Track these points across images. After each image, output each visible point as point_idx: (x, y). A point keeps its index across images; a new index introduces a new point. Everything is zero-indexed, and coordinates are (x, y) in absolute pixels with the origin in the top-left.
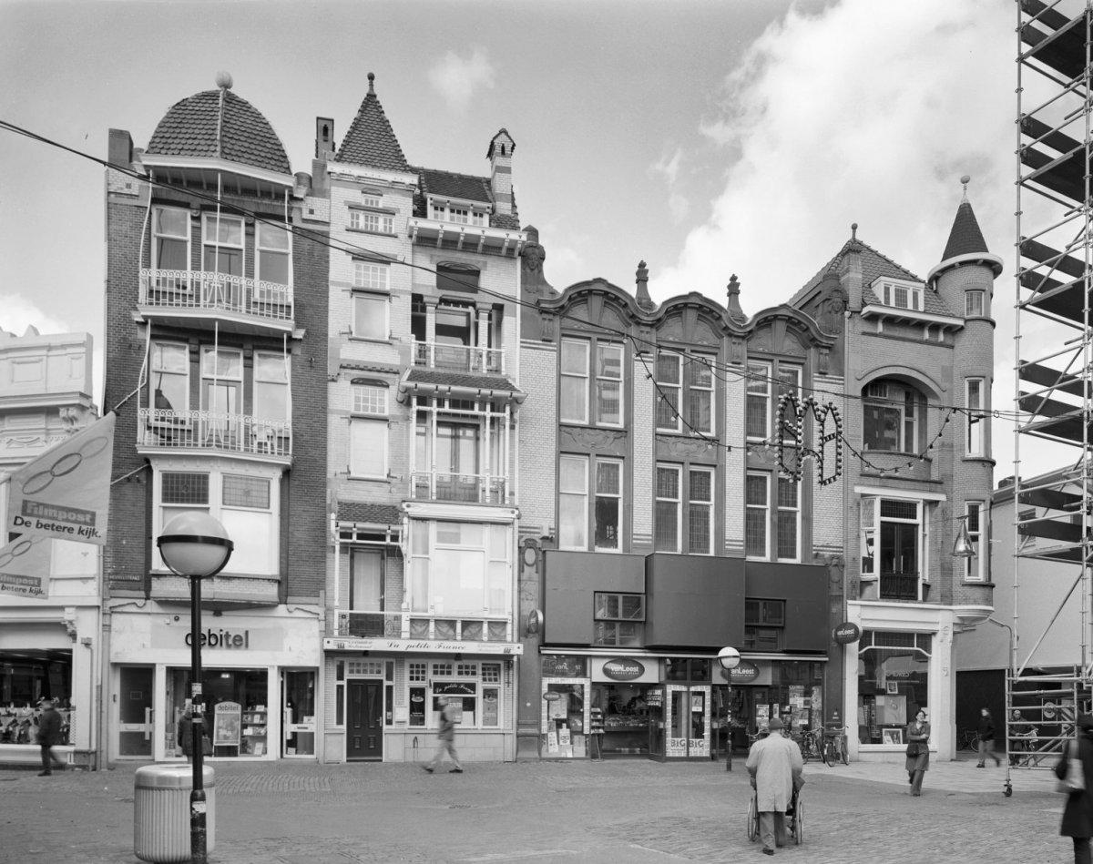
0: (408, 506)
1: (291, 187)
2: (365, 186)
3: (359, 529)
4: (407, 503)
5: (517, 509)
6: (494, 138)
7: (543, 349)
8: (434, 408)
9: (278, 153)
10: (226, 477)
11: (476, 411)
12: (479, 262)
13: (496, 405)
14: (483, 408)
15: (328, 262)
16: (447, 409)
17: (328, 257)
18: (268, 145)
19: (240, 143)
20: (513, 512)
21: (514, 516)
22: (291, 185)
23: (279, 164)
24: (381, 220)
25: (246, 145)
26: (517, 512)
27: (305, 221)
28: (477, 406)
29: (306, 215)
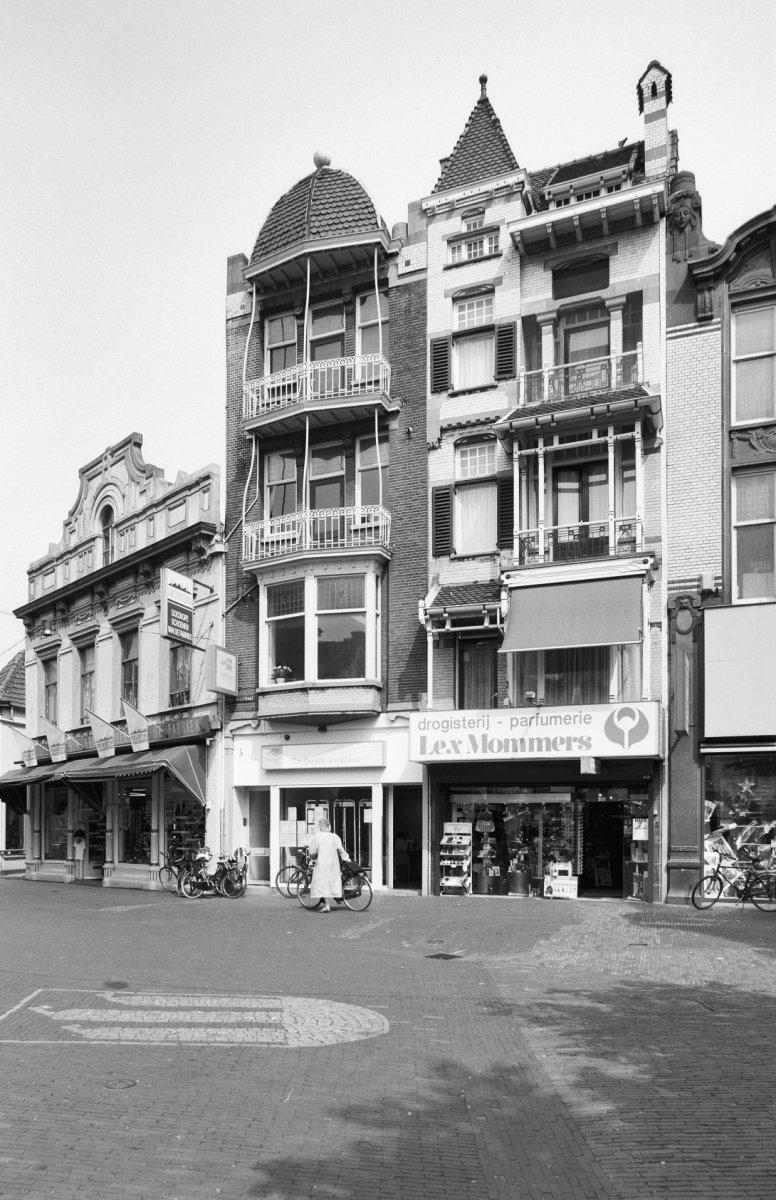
0: (508, 577)
1: (379, 243)
2: (465, 209)
3: (450, 614)
4: (506, 574)
5: (653, 556)
6: (641, 80)
7: (701, 333)
8: (541, 450)
9: (366, 211)
10: (321, 580)
11: (595, 439)
12: (606, 247)
13: (623, 422)
15: (425, 314)
16: (556, 445)
17: (425, 308)
18: (356, 207)
19: (327, 217)
20: (645, 562)
21: (647, 566)
22: (379, 240)
23: (367, 222)
24: (486, 243)
25: (334, 215)
26: (651, 561)
27: (401, 276)
28: (595, 434)
29: (403, 269)
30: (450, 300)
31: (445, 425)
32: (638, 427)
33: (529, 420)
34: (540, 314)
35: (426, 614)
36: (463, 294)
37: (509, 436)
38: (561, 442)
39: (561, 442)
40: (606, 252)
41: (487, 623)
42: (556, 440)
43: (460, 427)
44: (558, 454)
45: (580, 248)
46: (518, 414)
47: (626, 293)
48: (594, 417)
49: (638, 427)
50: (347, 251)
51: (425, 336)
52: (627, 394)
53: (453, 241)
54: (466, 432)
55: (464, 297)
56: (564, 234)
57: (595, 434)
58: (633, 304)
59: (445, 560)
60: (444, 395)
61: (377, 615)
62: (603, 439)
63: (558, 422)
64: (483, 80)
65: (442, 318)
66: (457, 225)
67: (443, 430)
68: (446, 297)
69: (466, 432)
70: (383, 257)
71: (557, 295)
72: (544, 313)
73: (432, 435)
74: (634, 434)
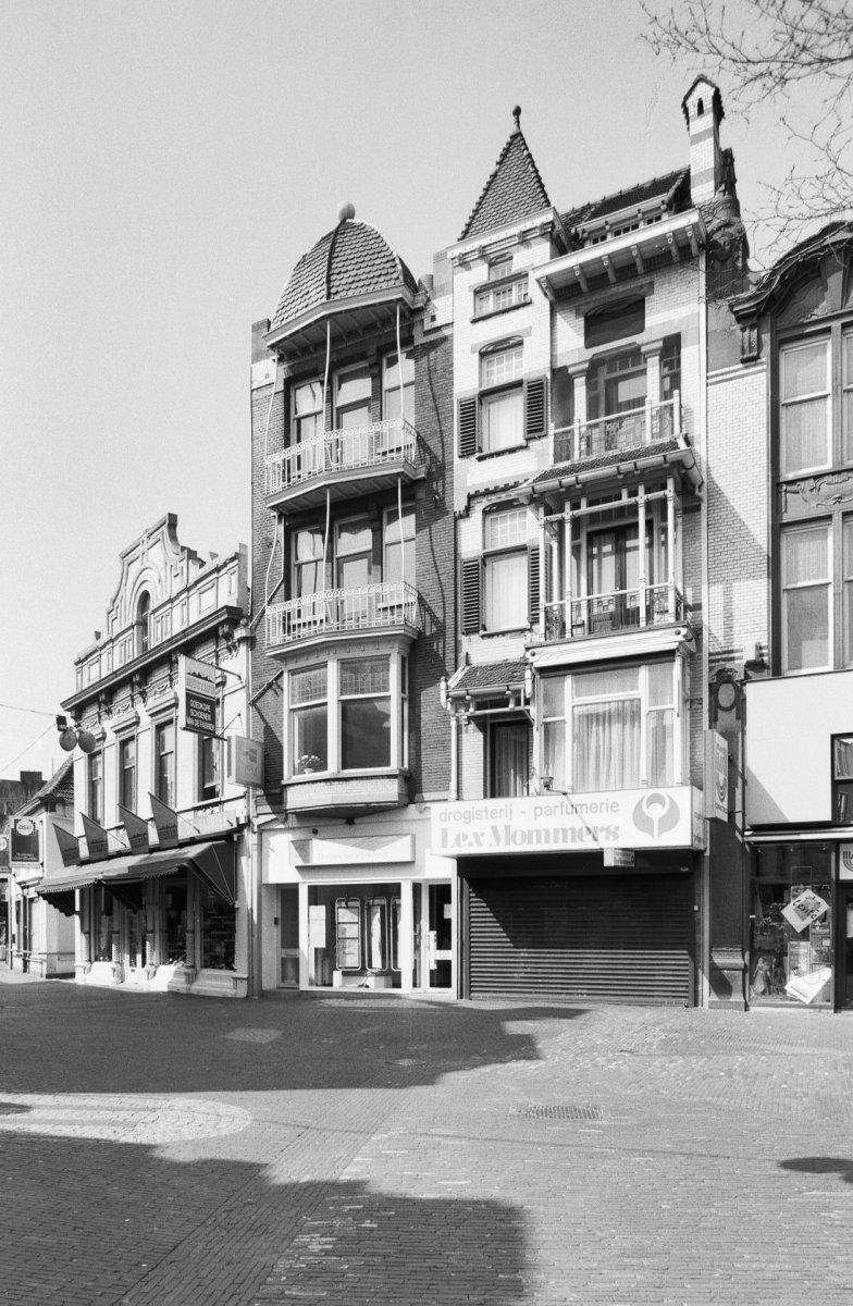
0: (534, 655)
1: (401, 299)
3: (474, 696)
4: (531, 651)
6: (686, 98)
7: (747, 375)
8: (568, 514)
10: (345, 665)
11: (625, 500)
12: (642, 287)
13: (654, 479)
14: (633, 494)
16: (584, 509)
17: (452, 365)
21: (680, 638)
22: (400, 296)
28: (625, 493)
29: (427, 327)
30: (477, 355)
31: (472, 492)
32: (670, 484)
33: (553, 483)
34: (572, 366)
35: (448, 697)
36: (491, 348)
37: (536, 499)
38: (590, 504)
39: (590, 504)
40: (641, 292)
41: (511, 706)
42: (584, 503)
43: (488, 493)
44: (593, 517)
45: (614, 289)
46: (544, 477)
47: (662, 336)
48: (621, 477)
49: (670, 484)
50: (369, 310)
51: (451, 396)
52: (660, 449)
53: (479, 292)
54: (494, 499)
55: (488, 353)
56: (595, 277)
57: (625, 493)
58: (671, 348)
59: (475, 637)
60: (473, 458)
61: (403, 699)
62: (633, 500)
63: (585, 484)
64: (517, 112)
65: (466, 379)
66: (480, 273)
67: (470, 498)
68: (473, 352)
69: (494, 499)
70: (407, 314)
71: (588, 345)
72: (575, 365)
73: (459, 504)
74: (667, 492)
